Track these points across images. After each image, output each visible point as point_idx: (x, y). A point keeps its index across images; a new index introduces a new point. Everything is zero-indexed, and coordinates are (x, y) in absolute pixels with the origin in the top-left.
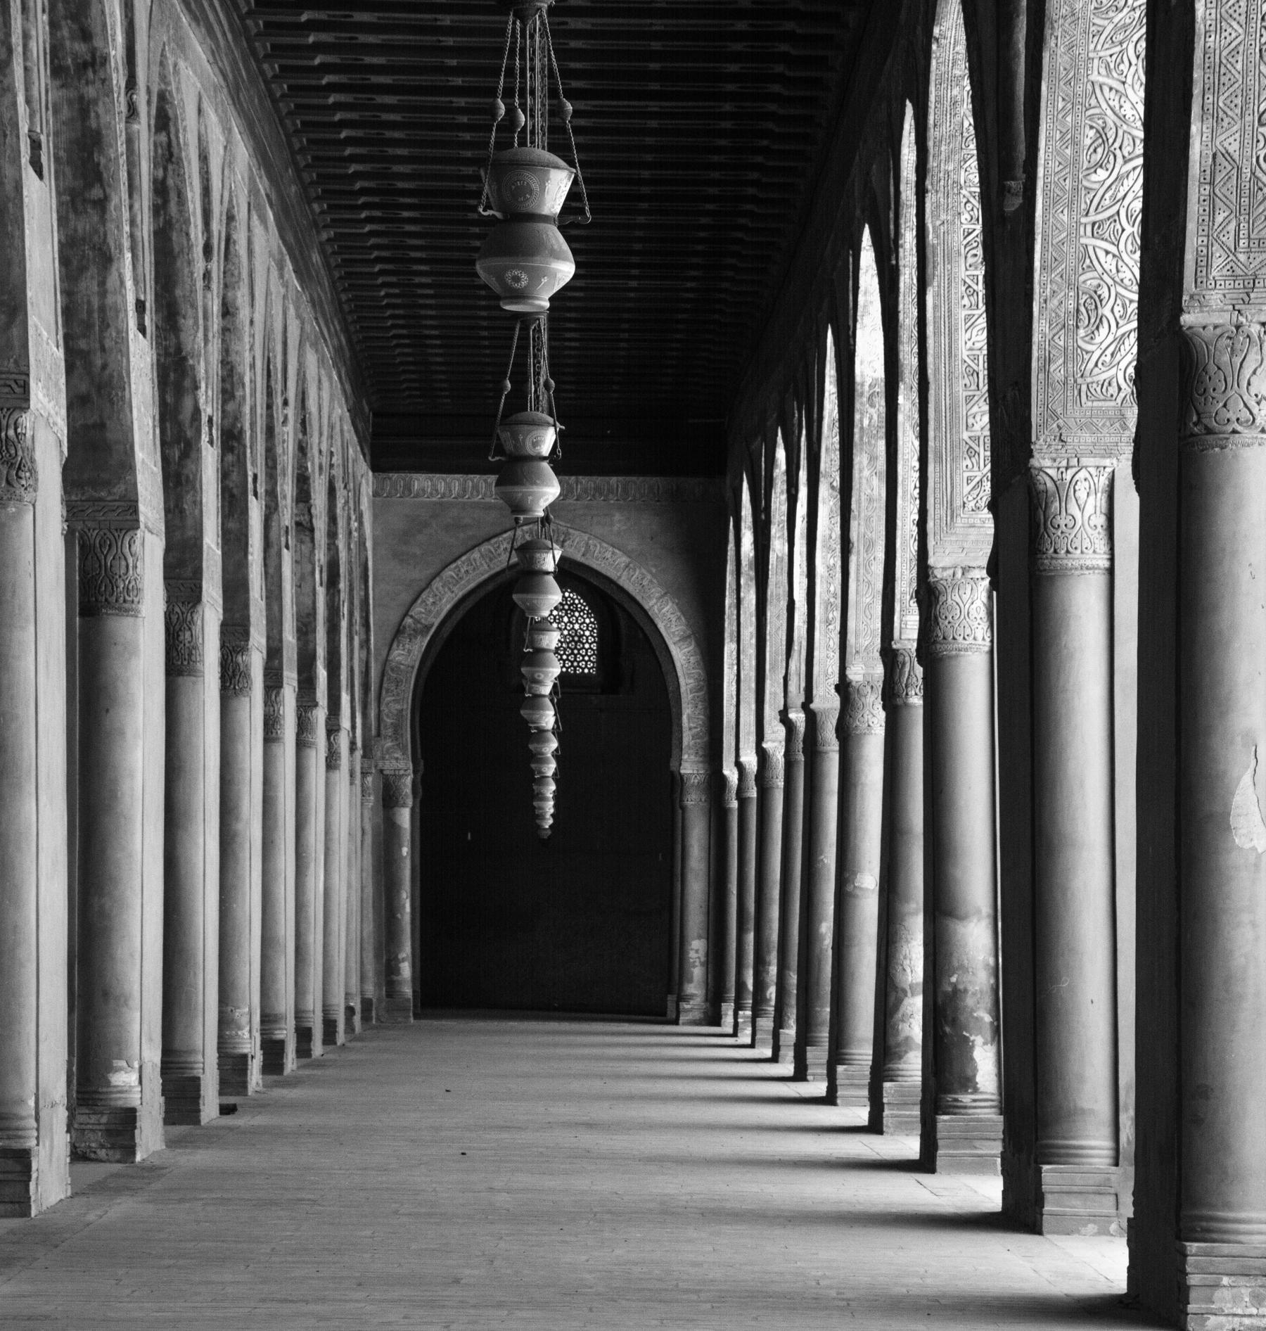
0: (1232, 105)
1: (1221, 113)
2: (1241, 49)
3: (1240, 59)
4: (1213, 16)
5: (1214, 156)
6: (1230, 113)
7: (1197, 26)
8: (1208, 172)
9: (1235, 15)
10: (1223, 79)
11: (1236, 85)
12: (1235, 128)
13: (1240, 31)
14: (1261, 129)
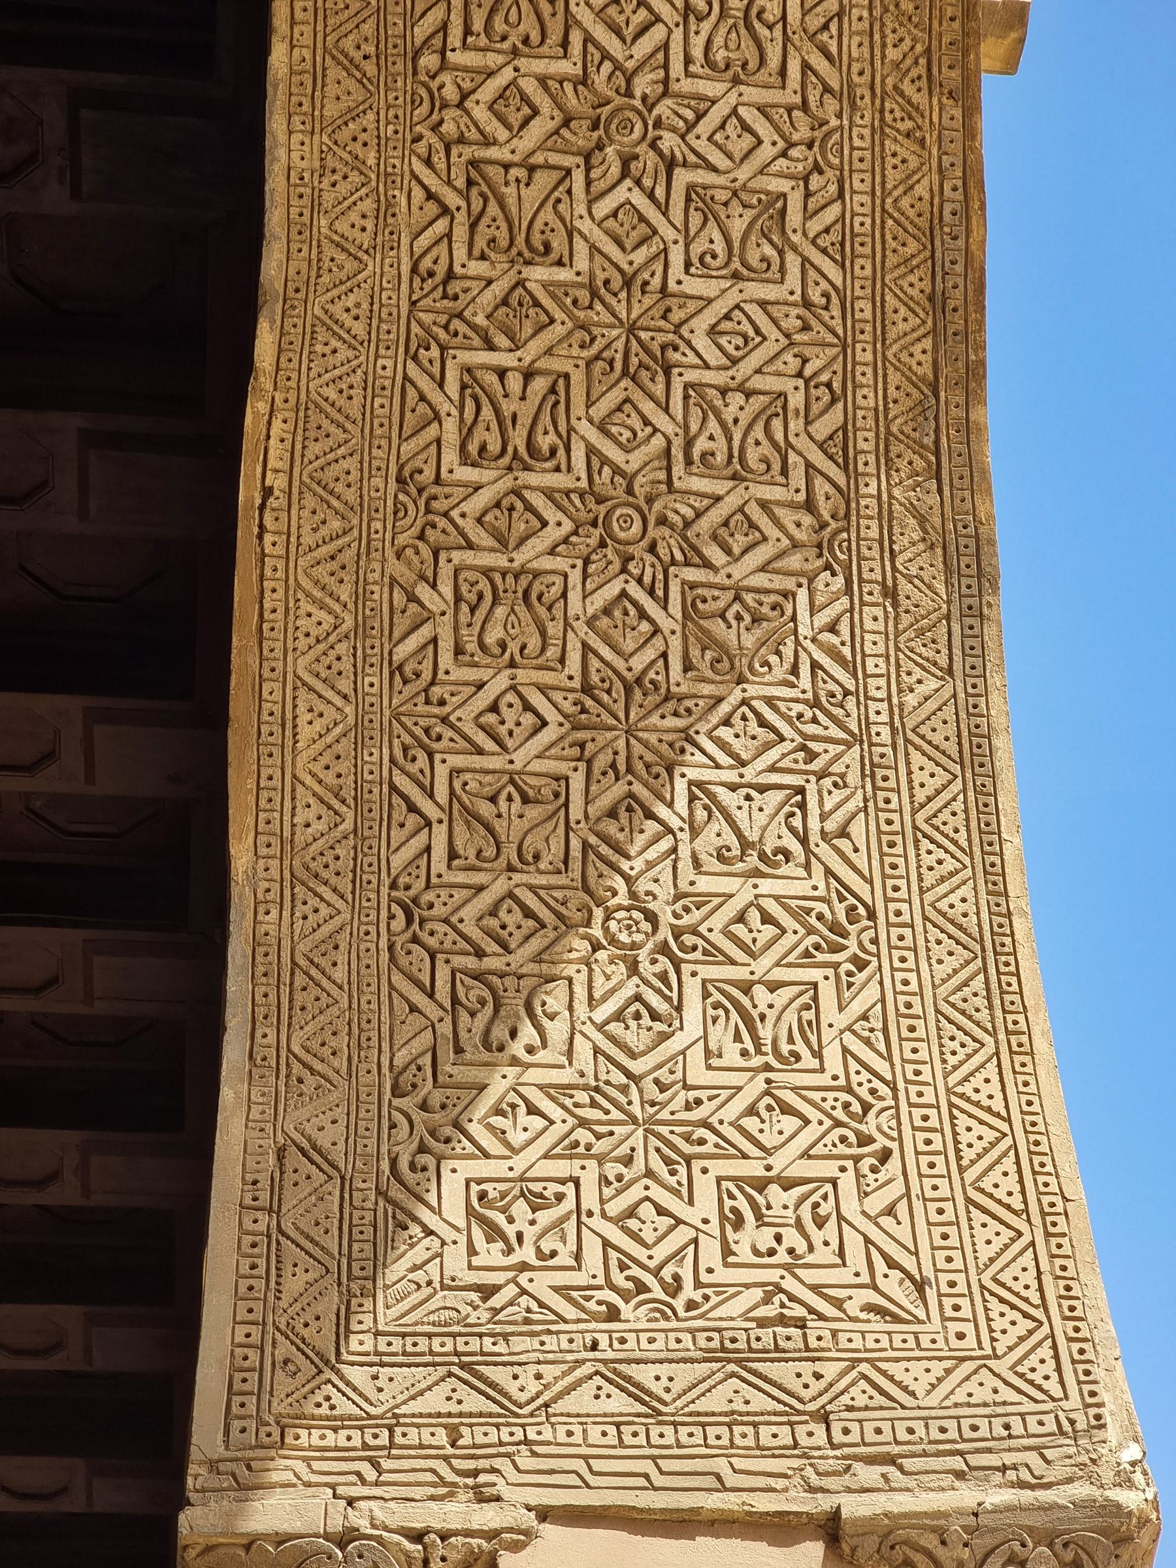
0: (326, 1052)
1: (296, 1067)
2: (343, 939)
3: (342, 958)
4: (275, 873)
5: (281, 1154)
6: (318, 1066)
7: (235, 891)
8: (265, 1183)
9: (325, 874)
10: (299, 997)
11: (334, 1010)
12: (334, 1096)
13: (340, 904)
14: (396, 1102)
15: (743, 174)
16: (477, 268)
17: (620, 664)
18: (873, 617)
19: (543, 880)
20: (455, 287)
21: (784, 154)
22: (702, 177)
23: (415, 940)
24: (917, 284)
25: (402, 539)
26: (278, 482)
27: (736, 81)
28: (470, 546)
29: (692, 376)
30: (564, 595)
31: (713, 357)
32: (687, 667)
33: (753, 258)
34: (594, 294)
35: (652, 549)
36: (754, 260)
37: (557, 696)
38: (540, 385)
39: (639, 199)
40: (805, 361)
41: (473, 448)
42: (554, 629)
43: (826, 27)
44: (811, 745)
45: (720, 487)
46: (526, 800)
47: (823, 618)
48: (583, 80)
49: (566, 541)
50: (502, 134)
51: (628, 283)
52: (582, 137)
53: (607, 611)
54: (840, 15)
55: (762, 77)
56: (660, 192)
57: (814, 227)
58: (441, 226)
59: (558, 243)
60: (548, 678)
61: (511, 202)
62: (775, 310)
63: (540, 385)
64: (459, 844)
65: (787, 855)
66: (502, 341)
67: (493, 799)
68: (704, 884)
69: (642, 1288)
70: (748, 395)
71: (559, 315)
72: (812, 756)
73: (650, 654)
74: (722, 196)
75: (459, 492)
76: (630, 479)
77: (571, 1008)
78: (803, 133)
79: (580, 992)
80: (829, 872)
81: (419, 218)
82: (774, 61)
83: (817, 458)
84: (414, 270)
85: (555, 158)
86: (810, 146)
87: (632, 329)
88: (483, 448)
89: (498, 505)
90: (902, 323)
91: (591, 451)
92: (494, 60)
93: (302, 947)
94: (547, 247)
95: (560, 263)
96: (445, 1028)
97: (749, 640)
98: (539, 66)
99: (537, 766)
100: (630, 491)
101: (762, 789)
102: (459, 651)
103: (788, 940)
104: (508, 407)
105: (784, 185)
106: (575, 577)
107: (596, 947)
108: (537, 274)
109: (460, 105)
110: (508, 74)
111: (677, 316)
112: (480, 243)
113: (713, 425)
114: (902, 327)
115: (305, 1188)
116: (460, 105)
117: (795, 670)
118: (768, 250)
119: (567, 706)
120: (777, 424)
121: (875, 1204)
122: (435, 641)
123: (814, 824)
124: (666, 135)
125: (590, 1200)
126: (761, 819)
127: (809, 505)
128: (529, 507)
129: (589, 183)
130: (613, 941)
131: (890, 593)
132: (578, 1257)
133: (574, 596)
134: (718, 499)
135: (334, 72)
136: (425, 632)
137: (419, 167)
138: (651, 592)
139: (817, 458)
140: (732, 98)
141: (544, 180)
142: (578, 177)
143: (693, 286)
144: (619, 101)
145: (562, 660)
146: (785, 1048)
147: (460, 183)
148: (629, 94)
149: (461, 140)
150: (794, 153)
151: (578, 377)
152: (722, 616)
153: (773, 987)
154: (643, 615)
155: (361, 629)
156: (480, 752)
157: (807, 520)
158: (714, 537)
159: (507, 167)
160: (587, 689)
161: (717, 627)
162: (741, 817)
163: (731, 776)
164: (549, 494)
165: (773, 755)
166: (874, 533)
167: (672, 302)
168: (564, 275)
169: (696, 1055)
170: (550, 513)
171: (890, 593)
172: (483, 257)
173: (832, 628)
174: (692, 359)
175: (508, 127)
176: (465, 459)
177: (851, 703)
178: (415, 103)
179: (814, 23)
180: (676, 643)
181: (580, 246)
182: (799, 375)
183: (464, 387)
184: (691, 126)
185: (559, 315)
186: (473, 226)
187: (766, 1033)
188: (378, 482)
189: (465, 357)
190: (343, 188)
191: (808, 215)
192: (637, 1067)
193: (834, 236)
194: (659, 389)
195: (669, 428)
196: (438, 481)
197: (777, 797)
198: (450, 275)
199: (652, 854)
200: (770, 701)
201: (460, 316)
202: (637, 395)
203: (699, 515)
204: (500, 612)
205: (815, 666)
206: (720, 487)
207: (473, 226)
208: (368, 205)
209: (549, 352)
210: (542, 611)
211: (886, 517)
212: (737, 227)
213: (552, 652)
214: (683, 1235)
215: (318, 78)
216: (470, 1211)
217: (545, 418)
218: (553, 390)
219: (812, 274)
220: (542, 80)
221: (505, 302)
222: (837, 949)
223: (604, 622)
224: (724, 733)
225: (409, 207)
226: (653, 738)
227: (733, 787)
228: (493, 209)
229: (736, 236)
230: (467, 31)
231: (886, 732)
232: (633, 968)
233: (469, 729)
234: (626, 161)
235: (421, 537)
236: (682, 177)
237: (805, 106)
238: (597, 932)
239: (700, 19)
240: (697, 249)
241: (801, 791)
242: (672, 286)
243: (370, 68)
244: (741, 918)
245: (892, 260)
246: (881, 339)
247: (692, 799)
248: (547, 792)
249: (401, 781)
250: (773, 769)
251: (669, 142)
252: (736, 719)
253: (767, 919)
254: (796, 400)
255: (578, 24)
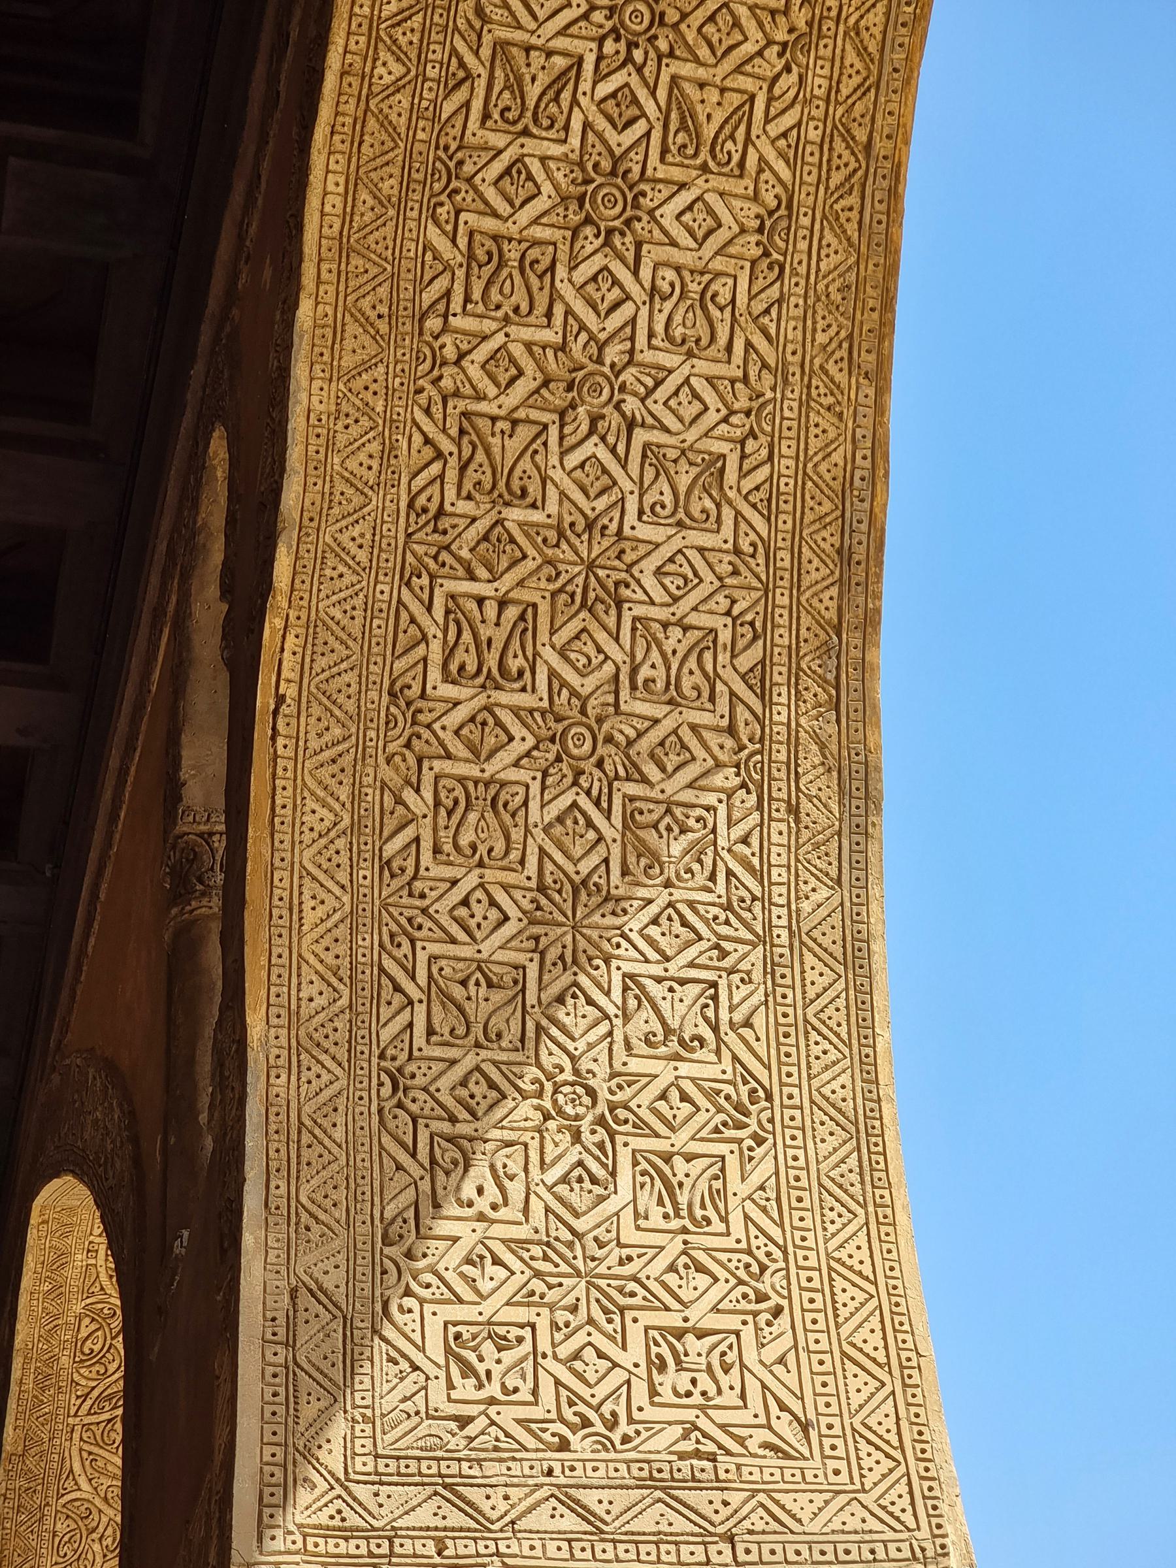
0: (328, 1203)
1: (304, 1216)
2: (341, 1103)
3: (340, 1120)
4: (283, 1041)
5: (294, 1294)
6: (322, 1216)
7: (251, 1055)
8: (282, 1321)
9: (326, 1044)
10: (305, 1152)
11: (335, 1167)
12: (337, 1244)
13: (338, 1071)
14: (387, 1250)
15: (691, 436)
16: (464, 507)
17: (570, 868)
18: (778, 832)
19: (503, 1057)
20: (444, 523)
21: (725, 420)
22: (657, 437)
23: (400, 1105)
24: (829, 539)
25: (392, 747)
26: (290, 691)
27: (690, 354)
28: (449, 756)
29: (639, 610)
30: (525, 803)
31: (658, 595)
32: (625, 872)
33: (695, 510)
34: (561, 534)
35: (600, 764)
36: (696, 514)
37: (518, 894)
38: (512, 612)
39: (603, 454)
40: (734, 602)
41: (453, 668)
42: (517, 835)
43: (767, 311)
44: (724, 944)
45: (658, 711)
46: (490, 985)
47: (738, 831)
48: (563, 348)
49: (528, 754)
50: (492, 391)
51: (590, 526)
52: (557, 397)
53: (560, 820)
54: (779, 301)
55: (711, 352)
56: (621, 449)
57: (748, 484)
58: (435, 468)
59: (534, 489)
60: (510, 878)
61: (496, 450)
62: (712, 557)
63: (512, 612)
64: (436, 1021)
65: (702, 1042)
66: (482, 573)
67: (464, 983)
68: (635, 1065)
69: (586, 1423)
70: (685, 629)
71: (531, 552)
72: (724, 954)
73: (594, 859)
74: (672, 454)
75: (441, 707)
76: (584, 701)
77: (526, 1170)
78: (742, 403)
79: (534, 1157)
80: (735, 1058)
81: (417, 461)
82: (722, 340)
83: (740, 688)
84: (411, 505)
85: (535, 415)
86: (748, 414)
87: (591, 566)
88: (462, 668)
89: (472, 719)
90: (815, 571)
91: (552, 674)
92: (488, 326)
93: (307, 1109)
94: (524, 492)
95: (533, 506)
96: (425, 1186)
97: (677, 849)
98: (527, 334)
99: (500, 956)
100: (583, 712)
101: (683, 982)
102: (437, 850)
103: (701, 1117)
104: (485, 632)
105: (723, 447)
106: (535, 787)
107: (547, 1117)
108: (515, 514)
109: (457, 363)
110: (500, 339)
111: (629, 557)
112: (468, 486)
113: (655, 655)
114: (815, 576)
115: (315, 1326)
116: (457, 363)
117: (712, 877)
118: (708, 504)
119: (529, 907)
120: (708, 656)
121: (771, 1353)
122: (417, 840)
123: (724, 1015)
124: (629, 399)
125: (544, 1345)
126: (681, 1008)
127: (731, 730)
128: (499, 723)
129: (562, 438)
130: (560, 1112)
131: (794, 810)
132: (535, 1392)
133: (534, 805)
134: (656, 721)
135: (352, 328)
136: (409, 833)
137: (420, 416)
138: (597, 803)
139: (740, 688)
140: (686, 370)
141: (525, 433)
142: (554, 431)
143: (644, 532)
144: (592, 367)
145: (522, 862)
146: (699, 1213)
147: (454, 432)
148: (600, 361)
149: (456, 394)
150: (734, 419)
151: (544, 608)
152: (655, 826)
153: (689, 1158)
154: (590, 824)
155: (356, 827)
156: (454, 941)
157: (729, 743)
158: (652, 755)
159: (494, 419)
160: (542, 889)
161: (650, 836)
162: (665, 1007)
163: (657, 970)
164: (515, 711)
165: (692, 952)
166: (783, 757)
167: (626, 545)
168: (537, 516)
169: (627, 1216)
170: (517, 730)
171: (794, 810)
172: (469, 497)
173: (745, 840)
174: (640, 595)
175: (498, 385)
176: (447, 678)
177: (757, 908)
178: (420, 360)
179: (758, 307)
180: (616, 850)
181: (552, 492)
182: (728, 613)
183: (448, 612)
184: (650, 392)
185: (531, 552)
186: (463, 469)
187: (683, 1199)
188: (373, 695)
189: (451, 586)
190: (355, 431)
191: (743, 475)
192: (580, 1225)
193: (762, 494)
194: (611, 622)
195: (619, 656)
196: (423, 695)
197: (693, 990)
198: (441, 512)
199: (592, 1036)
200: (691, 904)
201: (447, 548)
202: (593, 626)
203: (640, 735)
204: (473, 817)
205: (730, 873)
206: (658, 711)
207: (463, 469)
208: (375, 447)
209: (521, 583)
210: (507, 818)
211: (793, 743)
212: (683, 482)
213: (515, 855)
214: (618, 1376)
215: (338, 332)
216: (448, 1351)
217: (516, 644)
218: (522, 617)
219: (743, 526)
220: (528, 346)
221: (486, 538)
222: (741, 1126)
223: (558, 830)
224: (654, 931)
225: (410, 450)
226: (594, 934)
227: (659, 980)
228: (480, 456)
229: (682, 489)
230: (467, 300)
231: (785, 934)
232: (577, 1137)
233: (445, 920)
234: (594, 420)
235: (408, 745)
236: (641, 436)
237: (745, 379)
238: (547, 1104)
239: (664, 299)
240: (649, 499)
241: (714, 985)
242: (627, 531)
243: (383, 327)
244: (663, 1096)
245: (809, 517)
246: (797, 585)
247: (626, 988)
248: (508, 979)
249: (388, 963)
250: (692, 965)
251: (631, 405)
252: (663, 920)
253: (685, 1097)
254: (725, 636)
255: (561, 298)
